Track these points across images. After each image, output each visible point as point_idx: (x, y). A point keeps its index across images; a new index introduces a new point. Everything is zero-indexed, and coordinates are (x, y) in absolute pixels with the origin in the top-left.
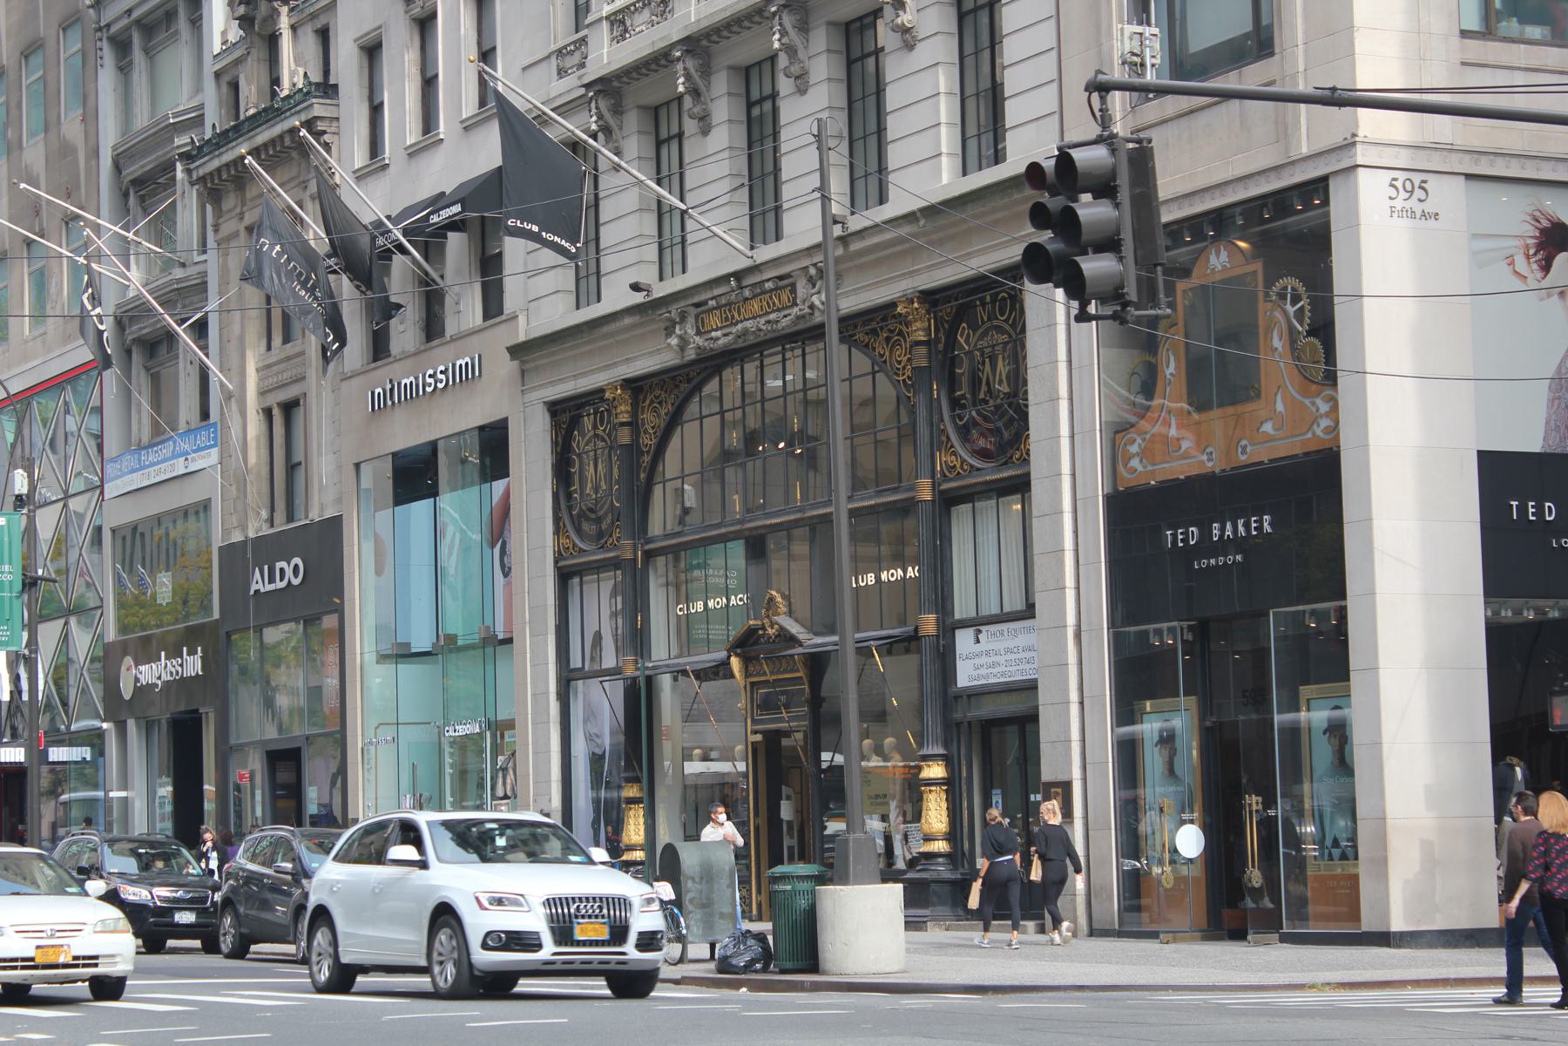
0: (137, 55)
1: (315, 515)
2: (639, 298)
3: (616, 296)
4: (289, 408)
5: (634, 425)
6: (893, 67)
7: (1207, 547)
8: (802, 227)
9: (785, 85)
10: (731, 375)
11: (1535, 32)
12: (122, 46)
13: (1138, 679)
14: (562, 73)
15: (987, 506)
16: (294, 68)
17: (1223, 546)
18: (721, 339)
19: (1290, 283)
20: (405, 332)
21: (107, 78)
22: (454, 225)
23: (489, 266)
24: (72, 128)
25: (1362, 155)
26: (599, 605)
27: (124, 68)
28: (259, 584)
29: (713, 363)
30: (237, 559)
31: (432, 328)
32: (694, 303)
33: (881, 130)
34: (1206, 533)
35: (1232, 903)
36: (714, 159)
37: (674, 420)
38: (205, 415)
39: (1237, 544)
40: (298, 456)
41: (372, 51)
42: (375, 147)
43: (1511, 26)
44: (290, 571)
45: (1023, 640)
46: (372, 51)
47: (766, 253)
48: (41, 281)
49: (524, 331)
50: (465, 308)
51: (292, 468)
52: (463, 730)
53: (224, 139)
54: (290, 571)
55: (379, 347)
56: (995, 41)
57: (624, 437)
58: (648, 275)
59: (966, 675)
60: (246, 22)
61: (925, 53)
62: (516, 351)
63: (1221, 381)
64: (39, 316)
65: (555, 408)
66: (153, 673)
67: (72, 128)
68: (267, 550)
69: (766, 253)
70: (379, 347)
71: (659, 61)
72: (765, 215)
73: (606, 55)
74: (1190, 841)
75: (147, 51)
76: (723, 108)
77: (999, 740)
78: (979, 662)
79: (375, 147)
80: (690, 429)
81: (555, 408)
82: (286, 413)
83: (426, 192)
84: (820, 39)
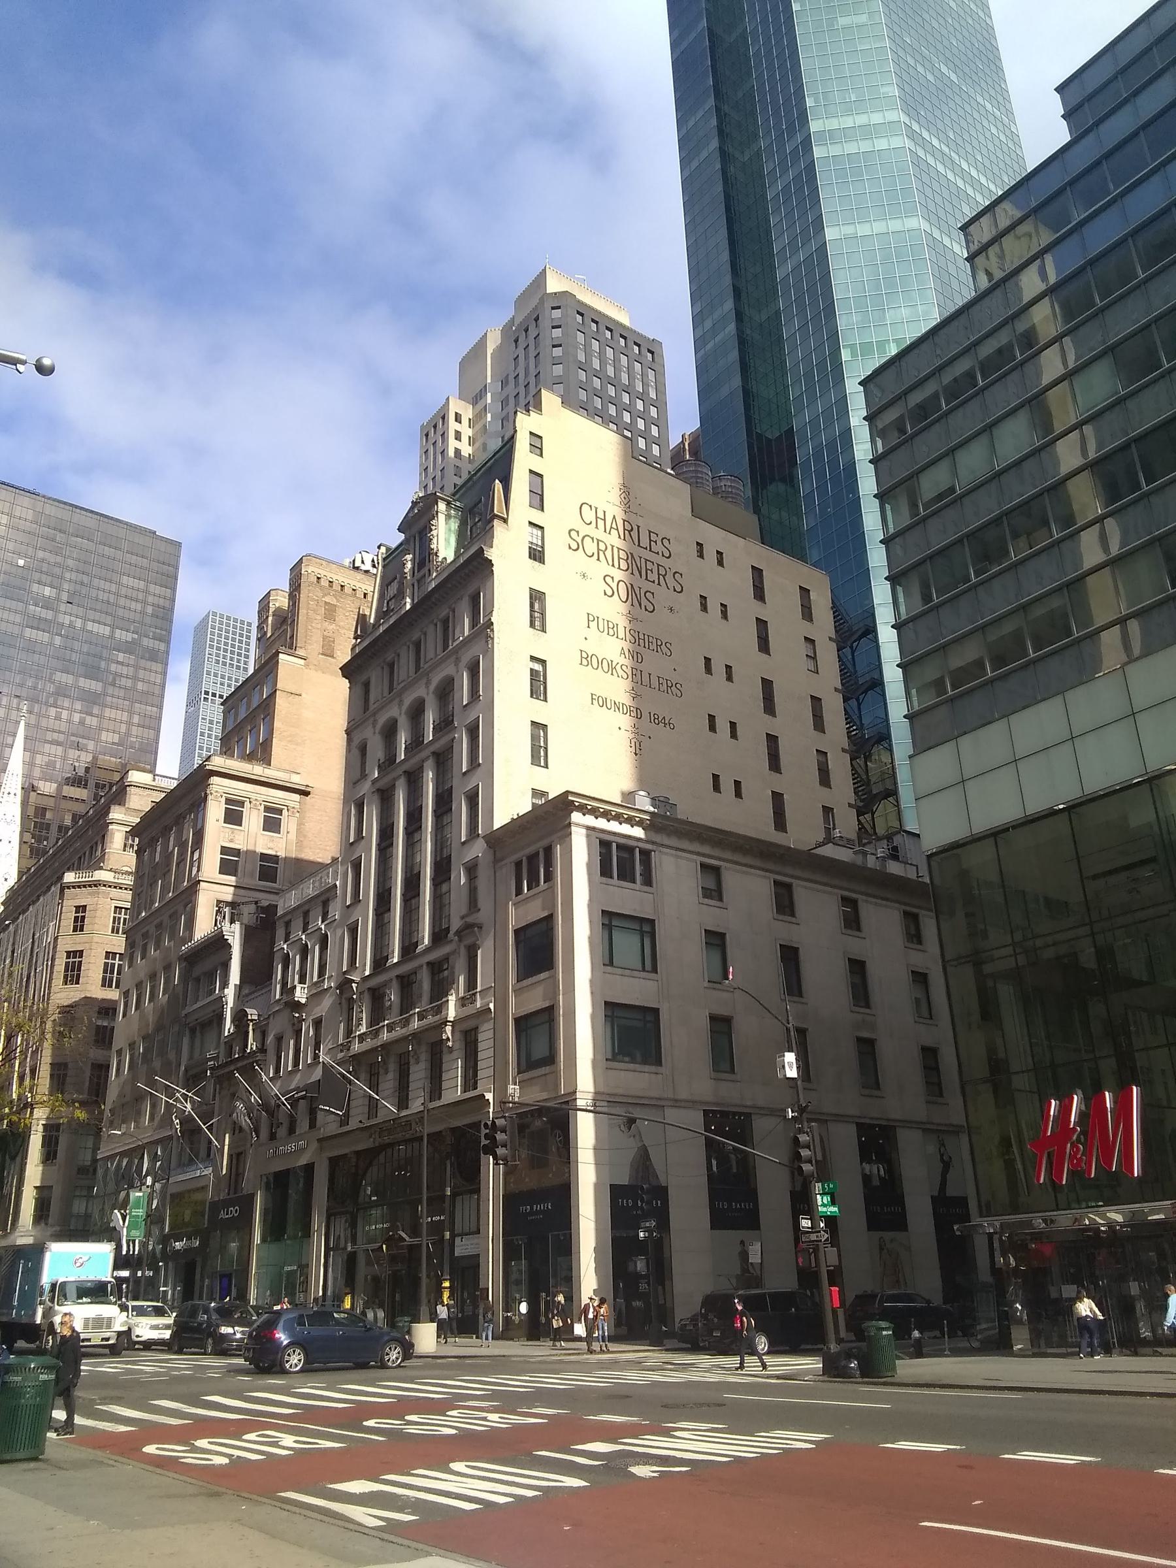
0: (198, 1034)
1: (245, 1192)
2: (362, 1125)
3: (353, 1124)
4: (239, 1155)
5: (357, 1166)
6: (446, 1058)
7: (532, 1213)
8: (416, 1106)
9: (412, 1061)
10: (389, 1151)
11: (627, 1059)
12: (193, 1031)
13: (510, 1253)
14: (342, 1051)
15: (466, 1197)
16: (252, 1045)
17: (537, 1213)
18: (386, 1140)
19: (558, 1132)
20: (282, 1132)
21: (186, 1041)
22: (303, 1098)
23: (313, 1112)
24: (172, 1056)
25: (578, 1095)
26: (341, 1226)
27: (192, 1038)
28: (223, 1215)
29: (383, 1148)
30: (215, 1207)
31: (292, 1130)
32: (381, 1129)
33: (441, 1076)
34: (532, 1208)
35: (535, 1329)
36: (389, 1082)
37: (371, 1164)
38: (209, 1155)
39: (541, 1212)
40: (241, 1171)
41: (279, 1039)
42: (277, 1070)
43: (620, 1057)
44: (234, 1211)
45: (476, 1241)
46: (279, 1039)
47: (404, 1113)
48: (153, 1106)
49: (324, 1132)
50: (303, 1125)
51: (237, 1175)
52: (290, 1268)
53: (227, 1064)
54: (234, 1211)
55: (273, 1136)
56: (476, 1053)
57: (353, 1170)
58: (364, 1118)
59: (458, 1252)
60: (236, 1027)
61: (455, 1054)
62: (319, 1140)
63: (538, 1163)
64: (152, 1118)
65: (331, 1159)
66: (178, 1245)
67: (172, 1056)
68: (226, 1204)
69: (404, 1113)
70: (273, 1136)
71: (374, 1050)
72: (403, 1103)
73: (356, 1047)
74: (524, 1308)
75: (202, 1034)
76: (392, 1066)
77: (467, 1274)
78: (463, 1248)
79: (277, 1070)
80: (375, 1169)
81: (331, 1159)
82: (237, 1157)
83: (292, 1087)
84: (424, 1048)
